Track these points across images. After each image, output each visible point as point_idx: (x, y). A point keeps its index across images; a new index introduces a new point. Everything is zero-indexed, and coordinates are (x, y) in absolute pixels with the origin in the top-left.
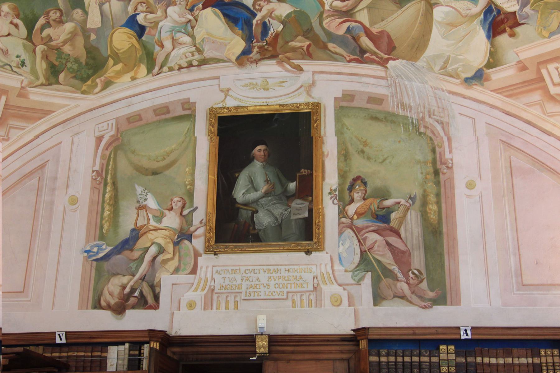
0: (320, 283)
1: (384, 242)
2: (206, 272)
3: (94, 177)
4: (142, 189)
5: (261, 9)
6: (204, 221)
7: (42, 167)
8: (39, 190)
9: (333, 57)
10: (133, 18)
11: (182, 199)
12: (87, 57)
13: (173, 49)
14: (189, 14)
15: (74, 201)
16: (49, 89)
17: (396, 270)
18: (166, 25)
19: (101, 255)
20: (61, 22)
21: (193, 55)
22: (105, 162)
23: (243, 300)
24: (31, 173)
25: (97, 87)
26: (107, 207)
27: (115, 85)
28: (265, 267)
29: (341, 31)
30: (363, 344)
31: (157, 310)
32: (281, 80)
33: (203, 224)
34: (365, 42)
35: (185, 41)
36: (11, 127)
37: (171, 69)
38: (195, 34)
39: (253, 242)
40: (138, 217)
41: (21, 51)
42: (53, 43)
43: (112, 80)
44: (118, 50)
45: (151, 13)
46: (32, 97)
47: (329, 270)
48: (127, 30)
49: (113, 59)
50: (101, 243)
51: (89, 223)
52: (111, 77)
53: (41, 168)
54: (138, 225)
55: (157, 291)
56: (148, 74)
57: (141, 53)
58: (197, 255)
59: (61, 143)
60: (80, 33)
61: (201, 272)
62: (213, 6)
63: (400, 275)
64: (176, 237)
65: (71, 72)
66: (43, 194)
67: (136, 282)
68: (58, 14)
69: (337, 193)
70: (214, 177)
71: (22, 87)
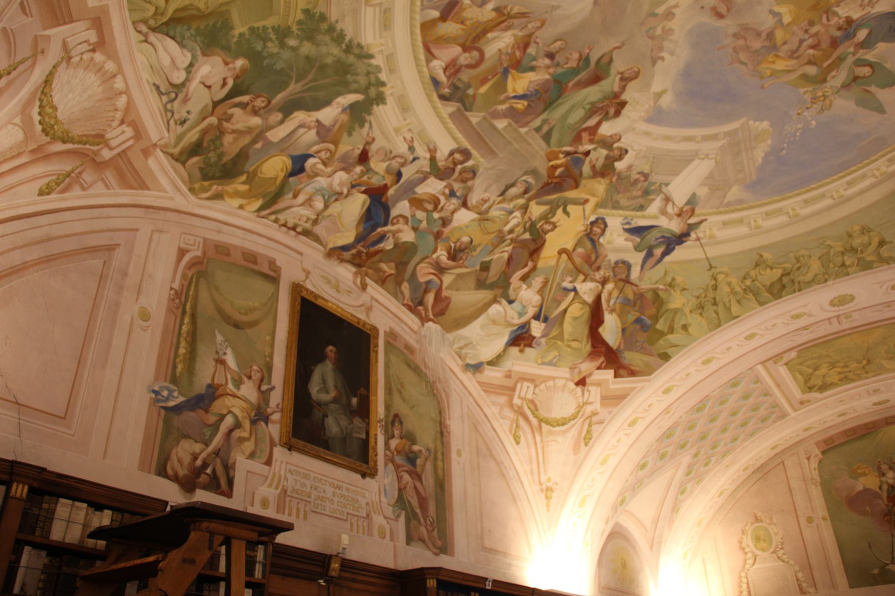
0: (372, 511)
1: (413, 485)
2: (280, 467)
3: (171, 296)
4: (223, 339)
6: (280, 406)
7: (111, 248)
8: (102, 279)
9: (396, 294)
11: (261, 370)
12: (232, 159)
14: (348, 188)
15: (145, 316)
16: (170, 162)
17: (420, 514)
19: (171, 404)
20: (255, 112)
21: (306, 222)
22: (186, 283)
23: (312, 511)
26: (183, 344)
27: (221, 202)
28: (331, 480)
29: (422, 279)
30: (432, 583)
31: (230, 499)
32: (349, 289)
33: (279, 410)
34: (430, 298)
36: (103, 180)
37: (276, 221)
38: (331, 207)
39: (324, 448)
40: (215, 371)
42: (225, 124)
44: (261, 173)
46: (151, 162)
47: (378, 500)
49: (248, 177)
50: (172, 387)
51: (160, 355)
52: (227, 192)
53: (108, 250)
54: (216, 382)
55: (231, 475)
56: (256, 211)
57: (273, 190)
58: (272, 444)
59: (137, 230)
60: (254, 134)
61: (276, 464)
62: (370, 197)
63: (422, 520)
64: (253, 414)
66: (108, 286)
67: (209, 455)
68: (263, 105)
69: (383, 423)
70: (294, 360)
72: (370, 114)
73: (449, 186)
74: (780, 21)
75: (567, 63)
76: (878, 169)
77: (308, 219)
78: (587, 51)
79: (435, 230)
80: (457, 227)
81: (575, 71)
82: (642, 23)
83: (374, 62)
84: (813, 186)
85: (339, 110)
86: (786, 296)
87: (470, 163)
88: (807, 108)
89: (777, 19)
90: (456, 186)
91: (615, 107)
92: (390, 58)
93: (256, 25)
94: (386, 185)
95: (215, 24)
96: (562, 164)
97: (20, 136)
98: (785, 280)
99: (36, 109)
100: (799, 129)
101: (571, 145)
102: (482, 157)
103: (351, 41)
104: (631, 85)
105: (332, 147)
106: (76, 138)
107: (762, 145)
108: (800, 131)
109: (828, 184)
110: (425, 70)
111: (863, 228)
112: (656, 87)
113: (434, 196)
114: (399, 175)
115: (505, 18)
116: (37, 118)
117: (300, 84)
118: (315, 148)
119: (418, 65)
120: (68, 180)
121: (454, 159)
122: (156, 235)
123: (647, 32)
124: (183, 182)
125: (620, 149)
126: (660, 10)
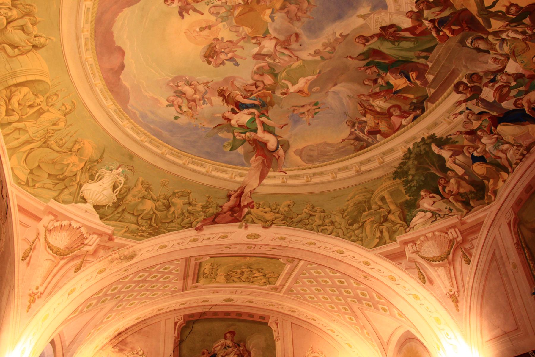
5: (522, 105)
10: (473, 157)
12: (474, 187)
13: (506, 155)
18: (489, 148)
20: (448, 182)
24: (492, 259)
25: (491, 197)
35: (507, 148)
37: (517, 164)
38: (507, 141)
41: (445, 205)
42: (454, 192)
43: (495, 189)
44: (483, 174)
45: (477, 148)
46: (469, 221)
48: (476, 164)
49: (486, 180)
51: (527, 276)
52: (493, 188)
56: (509, 174)
65: (474, 199)
68: (443, 180)
71: (460, 220)
72: (442, 138)
73: (486, 85)
74: (273, 12)
77: (517, 149)
78: (362, 68)
79: (527, 80)
80: (523, 68)
81: (378, 65)
82: (330, 58)
83: (411, 147)
85: (442, 151)
87: (465, 80)
89: (273, 15)
90: (485, 80)
91: (388, 30)
92: (407, 142)
93: (404, 192)
94: (489, 118)
95: (405, 206)
96: (448, 29)
97: (442, 268)
99: (434, 263)
101: (431, 33)
102: (458, 76)
103: (403, 159)
104: (367, 34)
105: (465, 148)
106: (449, 250)
110: (409, 125)
112: (361, 21)
113: (495, 91)
114: (481, 113)
115: (366, 110)
116: (437, 262)
117: (431, 169)
118: (467, 154)
119: (408, 130)
120: (466, 254)
121: (463, 90)
122: (500, 230)
123: (333, 53)
124: (483, 207)
125: (417, 6)
126: (318, 58)
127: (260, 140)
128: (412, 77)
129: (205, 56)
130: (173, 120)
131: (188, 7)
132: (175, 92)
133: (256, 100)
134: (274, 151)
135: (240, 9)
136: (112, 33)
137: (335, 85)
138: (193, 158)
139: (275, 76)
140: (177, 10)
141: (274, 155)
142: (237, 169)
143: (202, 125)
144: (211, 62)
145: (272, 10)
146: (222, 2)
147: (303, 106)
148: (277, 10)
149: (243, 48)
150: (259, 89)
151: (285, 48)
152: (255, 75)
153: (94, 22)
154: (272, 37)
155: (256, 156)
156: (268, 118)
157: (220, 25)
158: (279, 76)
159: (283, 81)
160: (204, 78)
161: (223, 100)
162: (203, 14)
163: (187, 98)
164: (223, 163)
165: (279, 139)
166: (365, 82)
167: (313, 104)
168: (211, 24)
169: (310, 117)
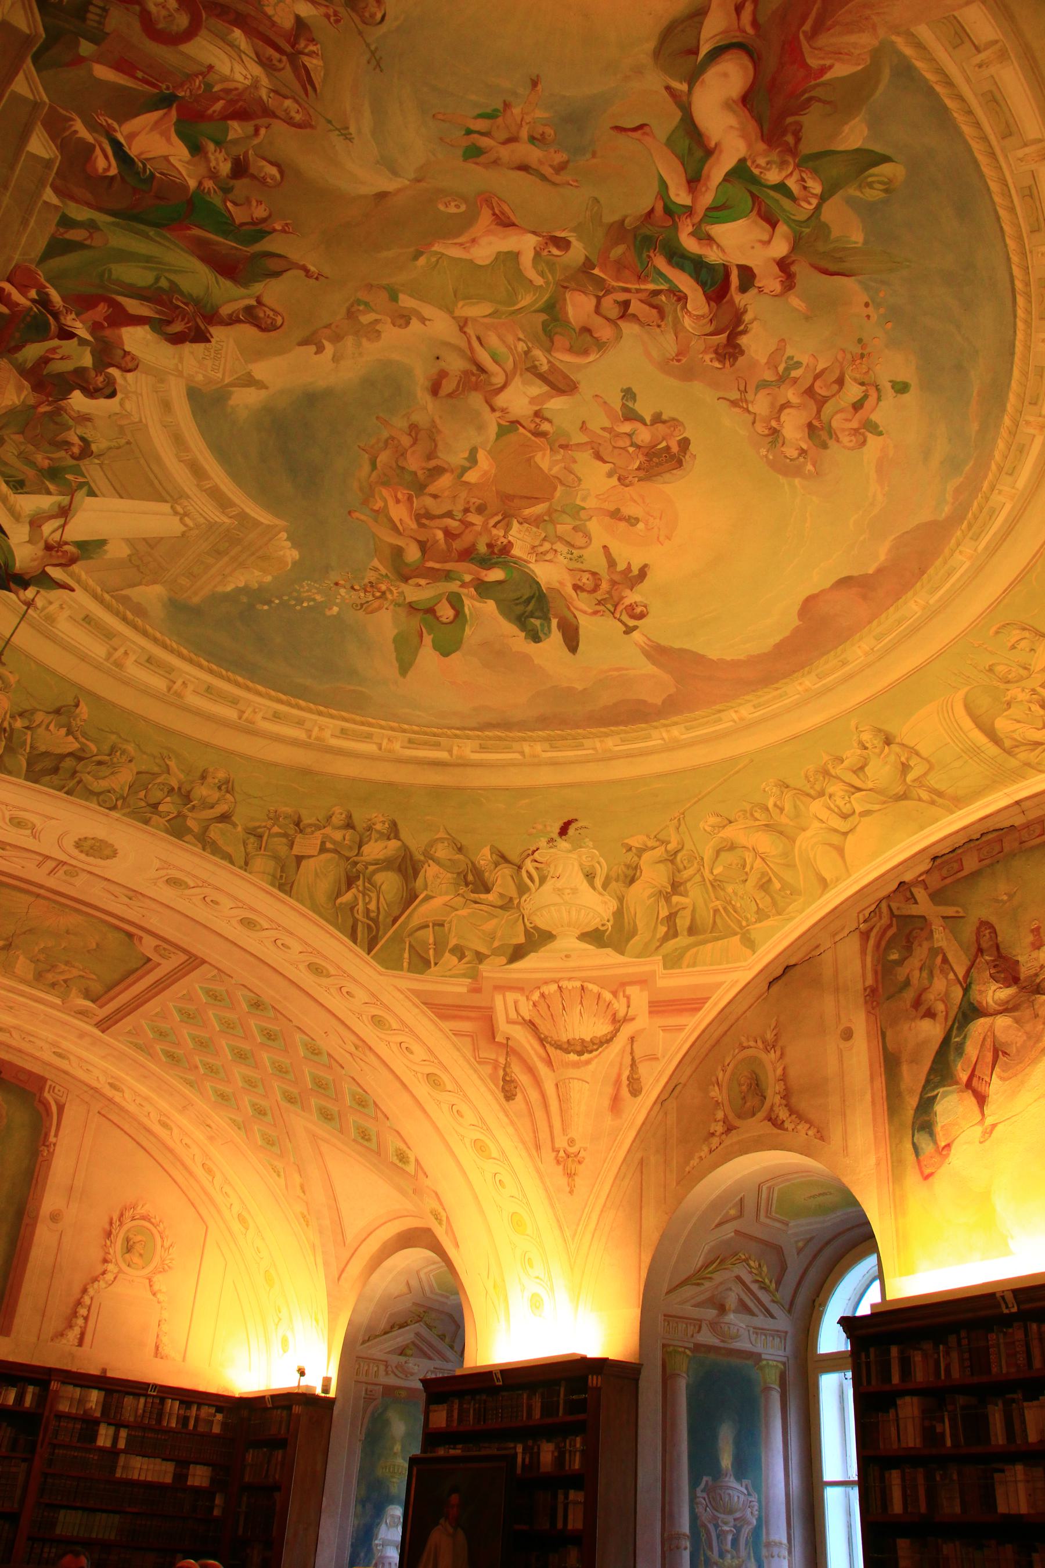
74: (464, 470)
75: (235, 204)
76: (321, 729)
78: (278, 227)
81: (226, 226)
82: (370, 287)
84: (240, 679)
86: (44, 786)
88: (352, 588)
89: (467, 464)
91: (189, 328)
96: (18, 304)
98: (68, 763)
100: (314, 600)
101: (64, 299)
104: (248, 331)
107: (257, 573)
108: (312, 603)
109: (259, 694)
111: (227, 782)
112: (261, 370)
115: (288, 49)
123: (358, 302)
125: (111, 382)
126: (406, 301)
127: (752, 126)
128: (106, 157)
129: (680, 464)
130: (913, 390)
131: (616, 578)
132: (825, 446)
133: (655, 267)
134: (740, 46)
135: (527, 512)
136: (778, 646)
137: (382, 196)
138: (1020, 238)
139: (553, 310)
140: (639, 587)
141: (750, 30)
142: (940, 71)
143: (871, 310)
144: (679, 442)
145: (462, 475)
146: (552, 544)
147: (524, 168)
148: (452, 471)
149: (583, 427)
150: (623, 297)
151: (482, 370)
152: (604, 340)
153: (776, 686)
154: (498, 414)
155: (823, 70)
156: (664, 185)
157: (591, 503)
158: (539, 304)
159: (539, 281)
160: (731, 421)
161: (744, 332)
162: (605, 547)
163: (819, 412)
164: (960, 134)
165: (684, 87)
166: (278, 177)
167: (481, 159)
168: (607, 519)
169: (516, 111)
